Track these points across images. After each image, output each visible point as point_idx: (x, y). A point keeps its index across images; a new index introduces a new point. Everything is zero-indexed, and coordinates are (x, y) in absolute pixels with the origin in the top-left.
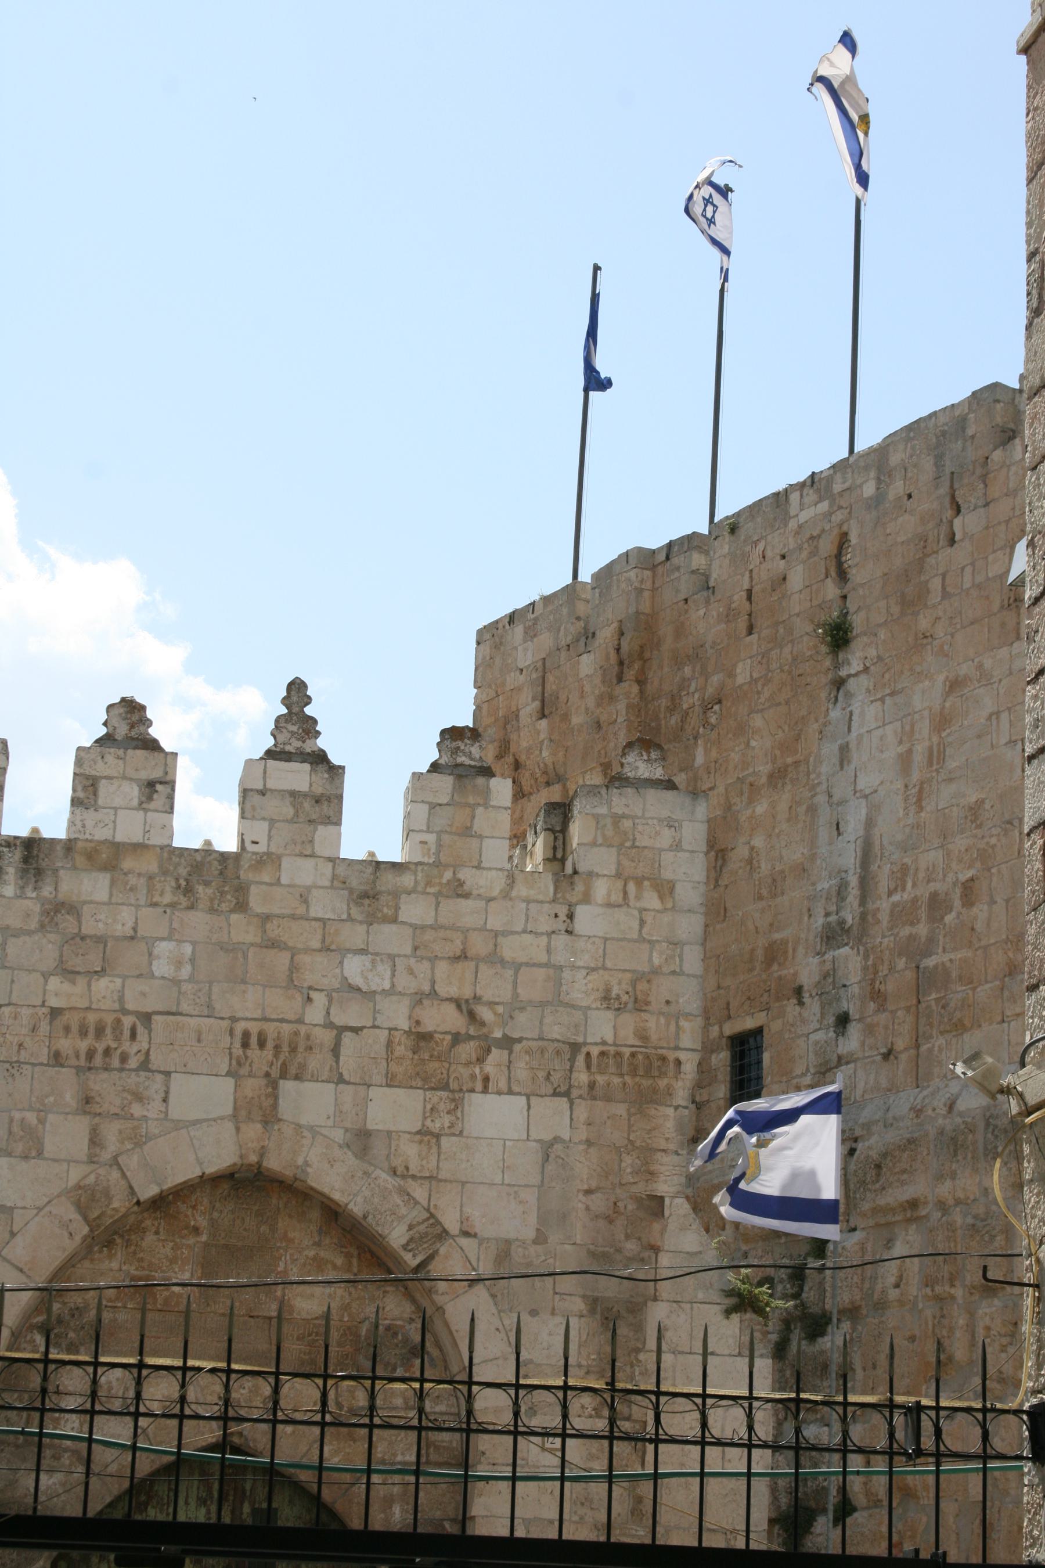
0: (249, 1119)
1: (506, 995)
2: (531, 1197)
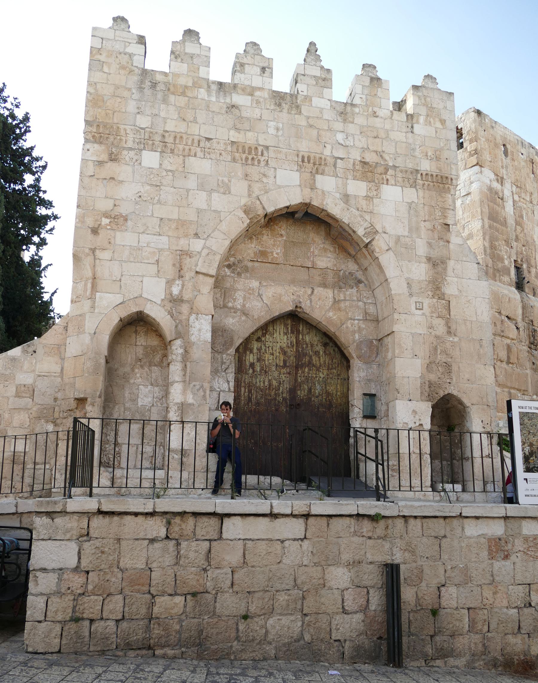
1: (393, 151)
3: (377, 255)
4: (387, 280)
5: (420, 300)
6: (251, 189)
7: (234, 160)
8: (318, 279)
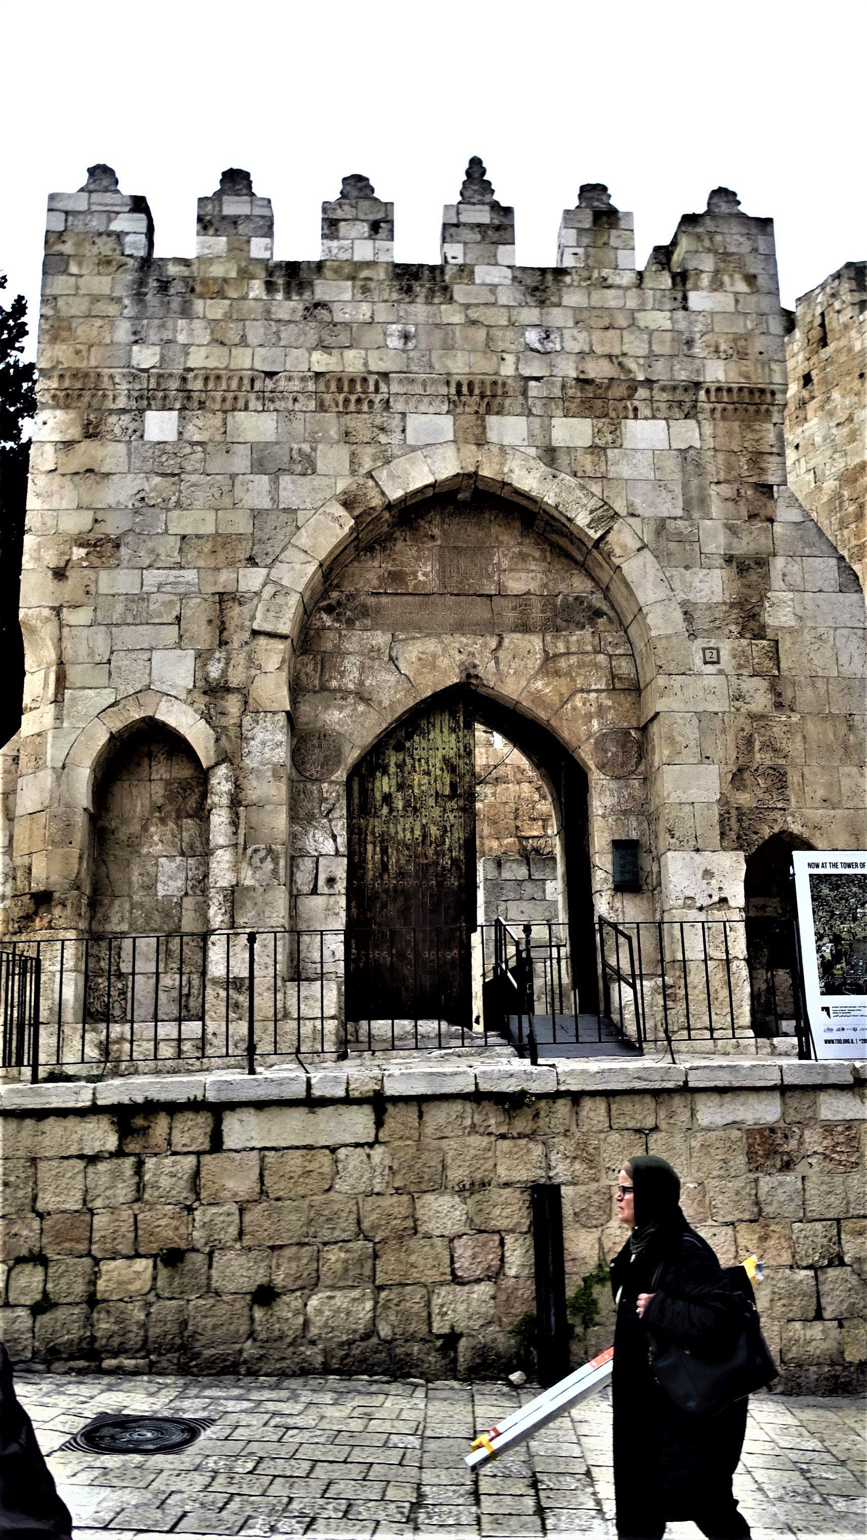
0: (466, 442)
1: (643, 351)
2: (678, 490)
3: (617, 561)
4: (640, 610)
5: (711, 645)
6: (356, 461)
7: (322, 407)
8: (510, 616)
